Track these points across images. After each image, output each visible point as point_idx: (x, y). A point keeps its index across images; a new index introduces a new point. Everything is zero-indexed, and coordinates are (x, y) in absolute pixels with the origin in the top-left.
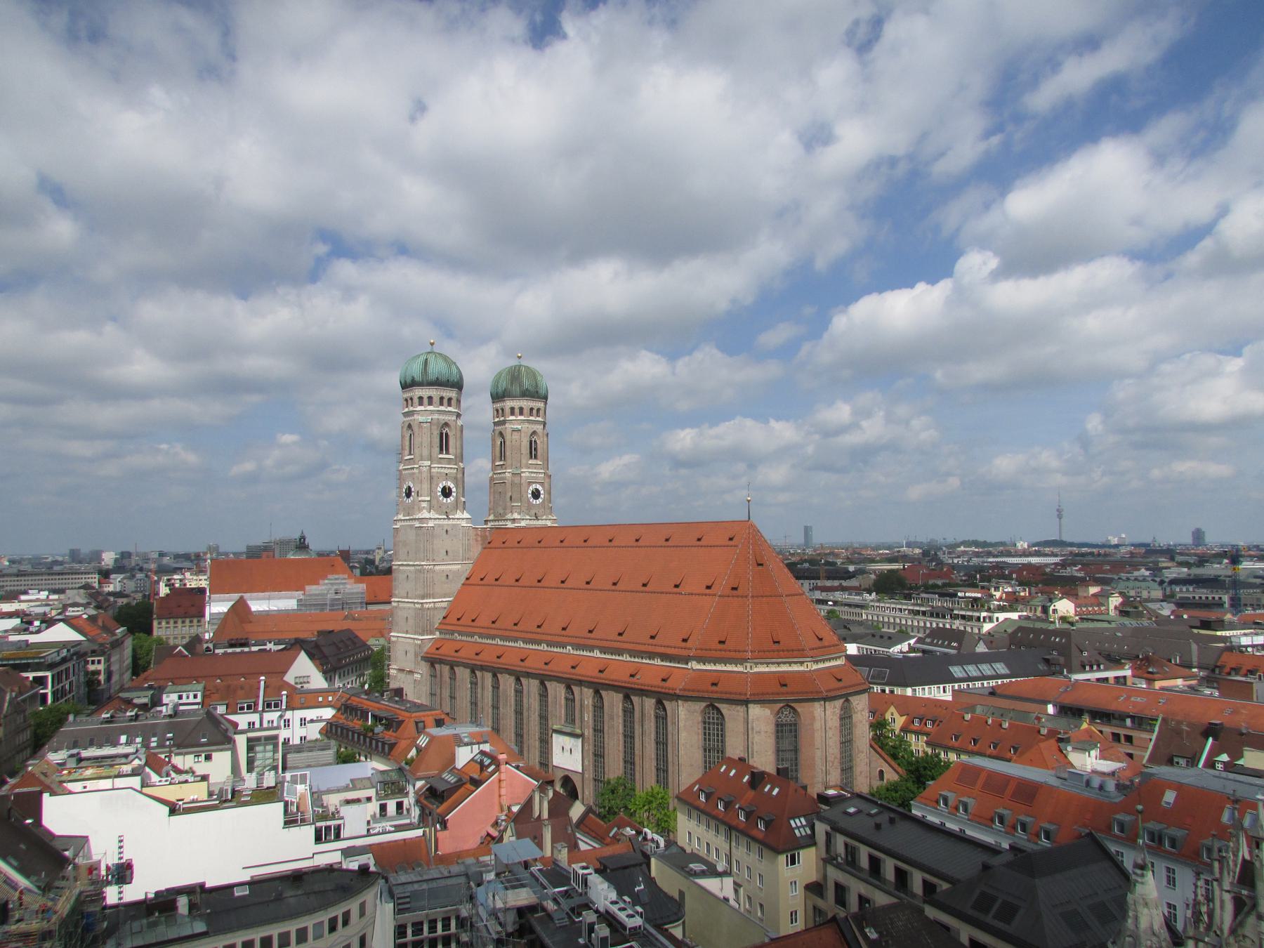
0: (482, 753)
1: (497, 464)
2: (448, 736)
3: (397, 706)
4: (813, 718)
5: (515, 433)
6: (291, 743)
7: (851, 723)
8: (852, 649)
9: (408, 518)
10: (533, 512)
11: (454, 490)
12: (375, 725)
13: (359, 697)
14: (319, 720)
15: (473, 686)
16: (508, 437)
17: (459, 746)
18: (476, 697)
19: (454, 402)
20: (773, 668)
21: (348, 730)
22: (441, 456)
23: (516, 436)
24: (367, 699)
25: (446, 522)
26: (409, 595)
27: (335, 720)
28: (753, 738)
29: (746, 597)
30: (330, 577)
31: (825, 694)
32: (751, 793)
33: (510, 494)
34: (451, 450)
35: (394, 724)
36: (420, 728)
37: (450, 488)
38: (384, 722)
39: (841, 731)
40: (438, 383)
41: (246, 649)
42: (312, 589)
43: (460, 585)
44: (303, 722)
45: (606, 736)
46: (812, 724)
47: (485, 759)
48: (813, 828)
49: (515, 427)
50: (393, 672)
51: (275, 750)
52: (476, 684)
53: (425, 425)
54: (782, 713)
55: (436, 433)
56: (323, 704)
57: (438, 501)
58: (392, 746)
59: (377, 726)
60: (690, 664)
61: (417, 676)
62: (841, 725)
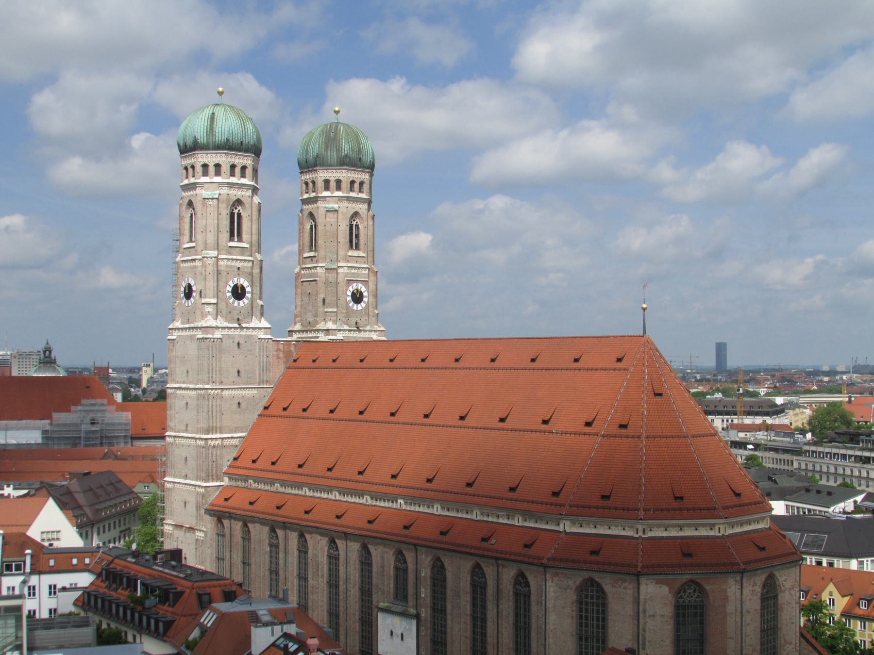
0: (286, 636)
1: (306, 255)
2: (241, 614)
3: (175, 573)
4: (726, 599)
5: (330, 215)
6: (37, 616)
7: (776, 605)
8: (779, 508)
9: (187, 326)
10: (353, 321)
11: (248, 289)
12: (145, 596)
13: (125, 560)
14: (73, 588)
15: (274, 549)
16: (320, 220)
17: (256, 627)
18: (277, 564)
19: (249, 172)
20: (674, 533)
21: (110, 602)
22: (231, 244)
23: (331, 218)
24: (134, 563)
25: (238, 332)
26: (189, 428)
27: (93, 588)
28: (645, 623)
29: (639, 437)
30: (84, 401)
31: (742, 566)
33: (322, 296)
34: (245, 236)
35: (171, 596)
36: (204, 602)
37: (243, 288)
38: (157, 592)
39: (762, 615)
40: (228, 146)
42: (61, 417)
43: (256, 416)
44: (53, 590)
45: (449, 617)
46: (725, 606)
47: (290, 644)
49: (330, 206)
50: (167, 529)
51: (18, 627)
52: (277, 546)
53: (210, 202)
54: (685, 592)
55: (225, 213)
56: (78, 568)
57: (227, 304)
58: (168, 625)
59: (148, 598)
60: (562, 526)
61: (201, 535)
62: (763, 608)
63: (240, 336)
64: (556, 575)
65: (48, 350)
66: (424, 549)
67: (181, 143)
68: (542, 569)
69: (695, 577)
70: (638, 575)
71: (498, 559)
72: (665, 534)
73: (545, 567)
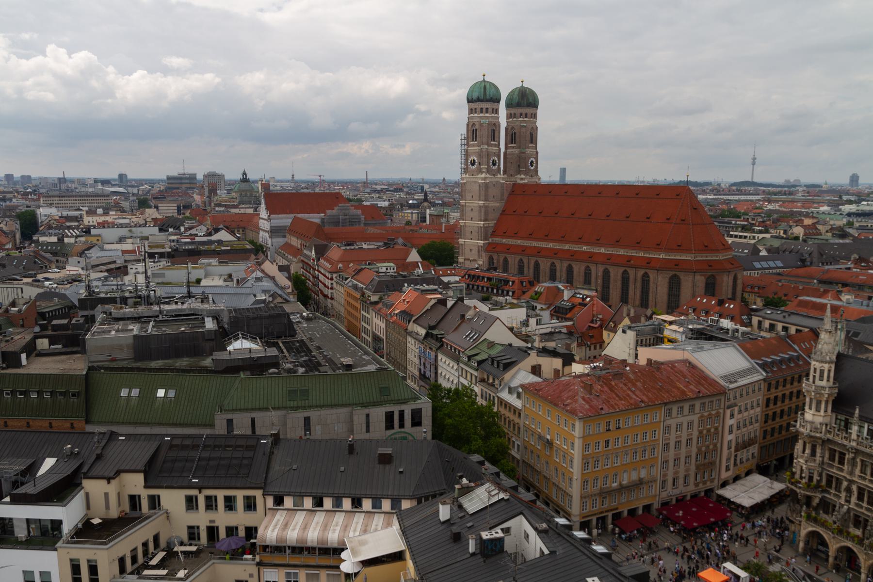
0: (576, 293)
2: (553, 287)
22: (492, 143)
23: (523, 130)
30: (340, 205)
32: (718, 308)
34: (496, 140)
41: (352, 247)
42: (329, 212)
43: (499, 215)
48: (750, 319)
63: (495, 181)
64: (662, 273)
65: (245, 174)
66: (600, 265)
67: (470, 98)
68: (656, 271)
69: (713, 274)
70: (695, 272)
71: (636, 267)
72: (701, 259)
73: (658, 270)
